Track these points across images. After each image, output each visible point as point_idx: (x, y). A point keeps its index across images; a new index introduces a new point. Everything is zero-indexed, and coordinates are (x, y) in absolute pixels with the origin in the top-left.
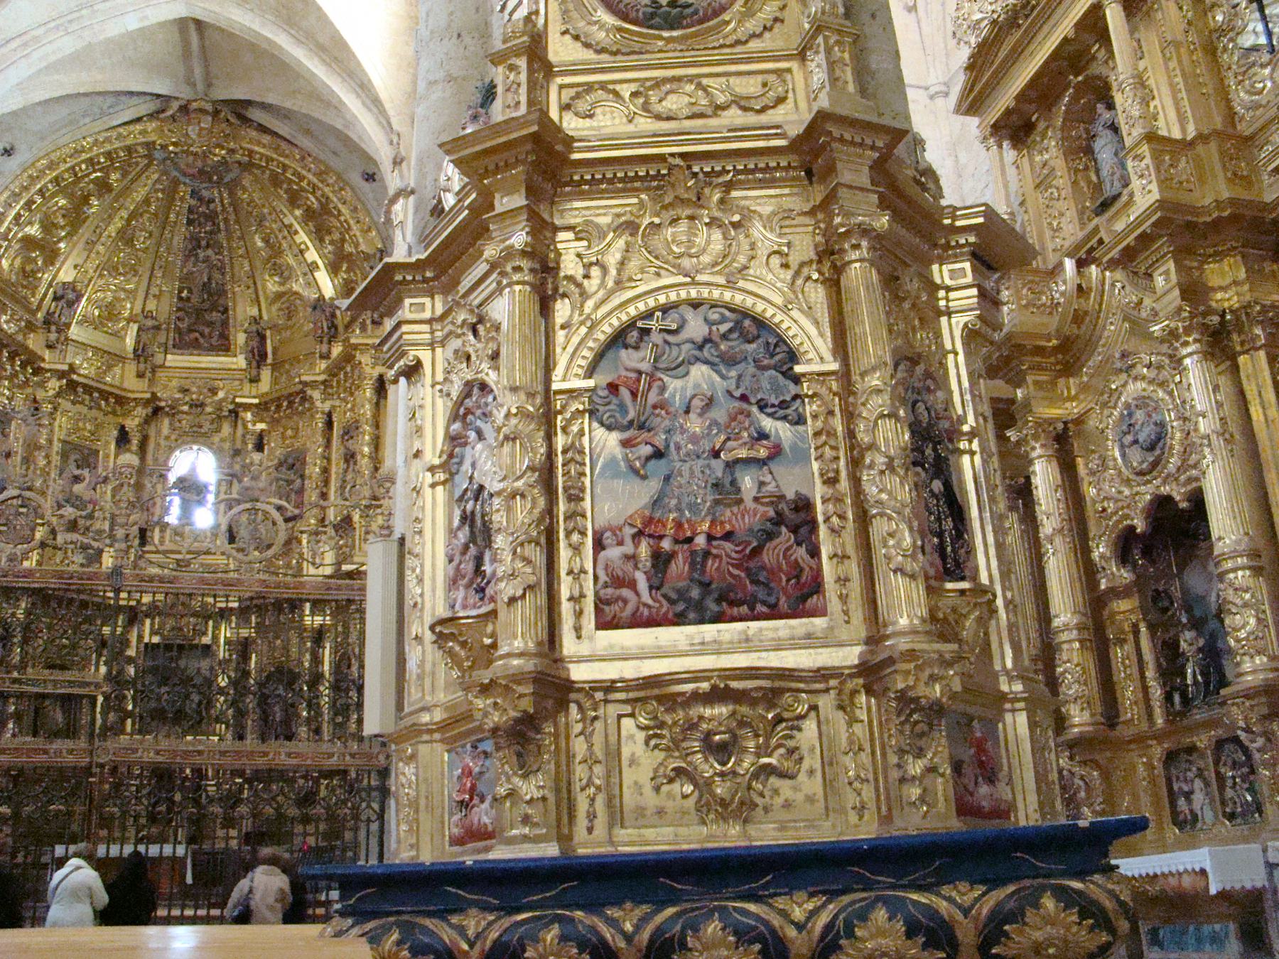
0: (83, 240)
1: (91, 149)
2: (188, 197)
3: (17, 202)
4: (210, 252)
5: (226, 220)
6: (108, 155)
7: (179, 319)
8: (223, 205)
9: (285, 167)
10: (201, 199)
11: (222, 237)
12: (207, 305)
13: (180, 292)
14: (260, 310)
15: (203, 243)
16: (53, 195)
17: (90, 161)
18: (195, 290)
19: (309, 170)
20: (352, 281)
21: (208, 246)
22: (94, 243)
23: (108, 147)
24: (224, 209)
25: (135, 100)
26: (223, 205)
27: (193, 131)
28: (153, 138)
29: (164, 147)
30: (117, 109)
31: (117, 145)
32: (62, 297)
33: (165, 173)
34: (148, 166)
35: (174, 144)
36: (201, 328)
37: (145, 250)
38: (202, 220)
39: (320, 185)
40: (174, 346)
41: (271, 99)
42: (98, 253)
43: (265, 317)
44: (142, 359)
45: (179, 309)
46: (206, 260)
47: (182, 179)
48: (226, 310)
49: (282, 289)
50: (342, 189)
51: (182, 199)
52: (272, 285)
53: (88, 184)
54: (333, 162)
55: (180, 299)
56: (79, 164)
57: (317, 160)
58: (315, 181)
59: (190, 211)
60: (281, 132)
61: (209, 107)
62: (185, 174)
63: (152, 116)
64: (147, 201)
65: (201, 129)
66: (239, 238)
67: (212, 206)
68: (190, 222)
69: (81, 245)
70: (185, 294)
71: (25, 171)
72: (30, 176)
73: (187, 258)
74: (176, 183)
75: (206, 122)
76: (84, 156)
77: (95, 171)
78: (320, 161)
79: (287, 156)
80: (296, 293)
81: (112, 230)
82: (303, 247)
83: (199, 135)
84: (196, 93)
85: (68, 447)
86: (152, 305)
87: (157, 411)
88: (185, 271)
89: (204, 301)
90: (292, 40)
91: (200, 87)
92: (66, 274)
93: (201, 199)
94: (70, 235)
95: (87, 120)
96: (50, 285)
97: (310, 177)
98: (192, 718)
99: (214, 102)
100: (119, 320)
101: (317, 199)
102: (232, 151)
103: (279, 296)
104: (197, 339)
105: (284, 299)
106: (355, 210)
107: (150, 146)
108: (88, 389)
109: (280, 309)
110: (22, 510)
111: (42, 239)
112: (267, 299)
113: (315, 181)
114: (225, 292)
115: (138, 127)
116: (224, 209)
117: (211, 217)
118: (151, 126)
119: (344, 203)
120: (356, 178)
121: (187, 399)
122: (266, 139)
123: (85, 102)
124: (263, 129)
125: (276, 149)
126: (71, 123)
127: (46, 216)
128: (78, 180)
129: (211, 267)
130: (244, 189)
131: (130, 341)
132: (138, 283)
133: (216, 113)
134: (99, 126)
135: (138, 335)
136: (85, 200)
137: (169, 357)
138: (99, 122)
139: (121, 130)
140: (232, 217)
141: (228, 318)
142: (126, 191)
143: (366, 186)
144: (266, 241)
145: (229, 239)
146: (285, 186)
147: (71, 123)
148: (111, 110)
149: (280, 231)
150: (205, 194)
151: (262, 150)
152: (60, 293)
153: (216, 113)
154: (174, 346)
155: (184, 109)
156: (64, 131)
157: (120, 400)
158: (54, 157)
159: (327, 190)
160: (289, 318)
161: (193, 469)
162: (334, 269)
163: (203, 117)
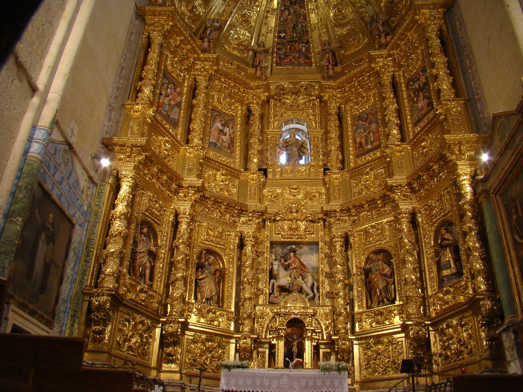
7: (279, 49)
36: (293, 54)
44: (259, 68)
45: (278, 44)
48: (307, 43)
73: (282, 12)
85: (216, 113)
98: (307, 294)
104: (291, 60)
114: (307, 31)
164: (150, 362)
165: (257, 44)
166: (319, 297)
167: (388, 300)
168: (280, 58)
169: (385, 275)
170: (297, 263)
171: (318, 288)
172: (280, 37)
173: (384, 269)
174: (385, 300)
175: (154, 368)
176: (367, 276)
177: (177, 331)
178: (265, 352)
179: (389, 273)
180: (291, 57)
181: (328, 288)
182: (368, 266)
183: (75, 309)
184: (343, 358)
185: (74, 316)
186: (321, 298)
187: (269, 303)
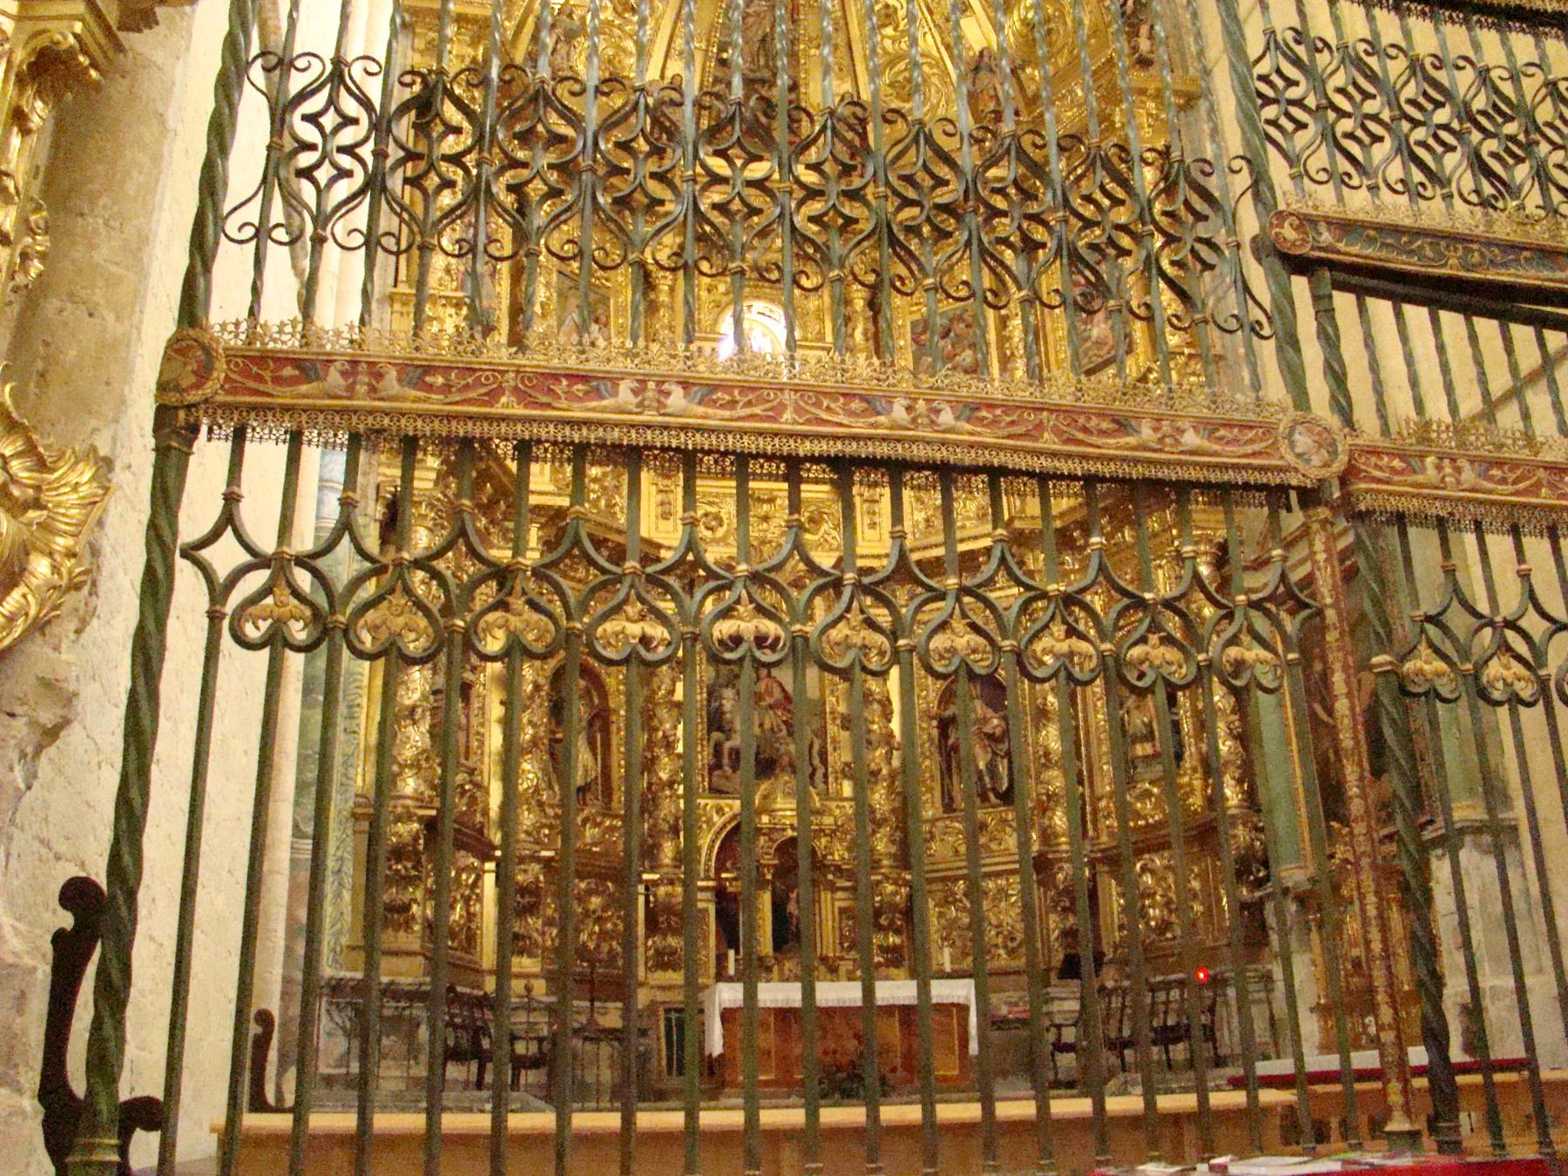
164: (477, 958)
165: (662, 77)
166: (826, 776)
167: (998, 795)
169: (990, 736)
170: (777, 694)
171: (823, 756)
173: (985, 720)
174: (992, 796)
175: (490, 972)
176: (944, 735)
177: (537, 879)
178: (706, 910)
179: (998, 731)
181: (847, 757)
182: (948, 713)
183: (339, 853)
184: (892, 922)
185: (339, 871)
186: (831, 779)
187: (710, 788)
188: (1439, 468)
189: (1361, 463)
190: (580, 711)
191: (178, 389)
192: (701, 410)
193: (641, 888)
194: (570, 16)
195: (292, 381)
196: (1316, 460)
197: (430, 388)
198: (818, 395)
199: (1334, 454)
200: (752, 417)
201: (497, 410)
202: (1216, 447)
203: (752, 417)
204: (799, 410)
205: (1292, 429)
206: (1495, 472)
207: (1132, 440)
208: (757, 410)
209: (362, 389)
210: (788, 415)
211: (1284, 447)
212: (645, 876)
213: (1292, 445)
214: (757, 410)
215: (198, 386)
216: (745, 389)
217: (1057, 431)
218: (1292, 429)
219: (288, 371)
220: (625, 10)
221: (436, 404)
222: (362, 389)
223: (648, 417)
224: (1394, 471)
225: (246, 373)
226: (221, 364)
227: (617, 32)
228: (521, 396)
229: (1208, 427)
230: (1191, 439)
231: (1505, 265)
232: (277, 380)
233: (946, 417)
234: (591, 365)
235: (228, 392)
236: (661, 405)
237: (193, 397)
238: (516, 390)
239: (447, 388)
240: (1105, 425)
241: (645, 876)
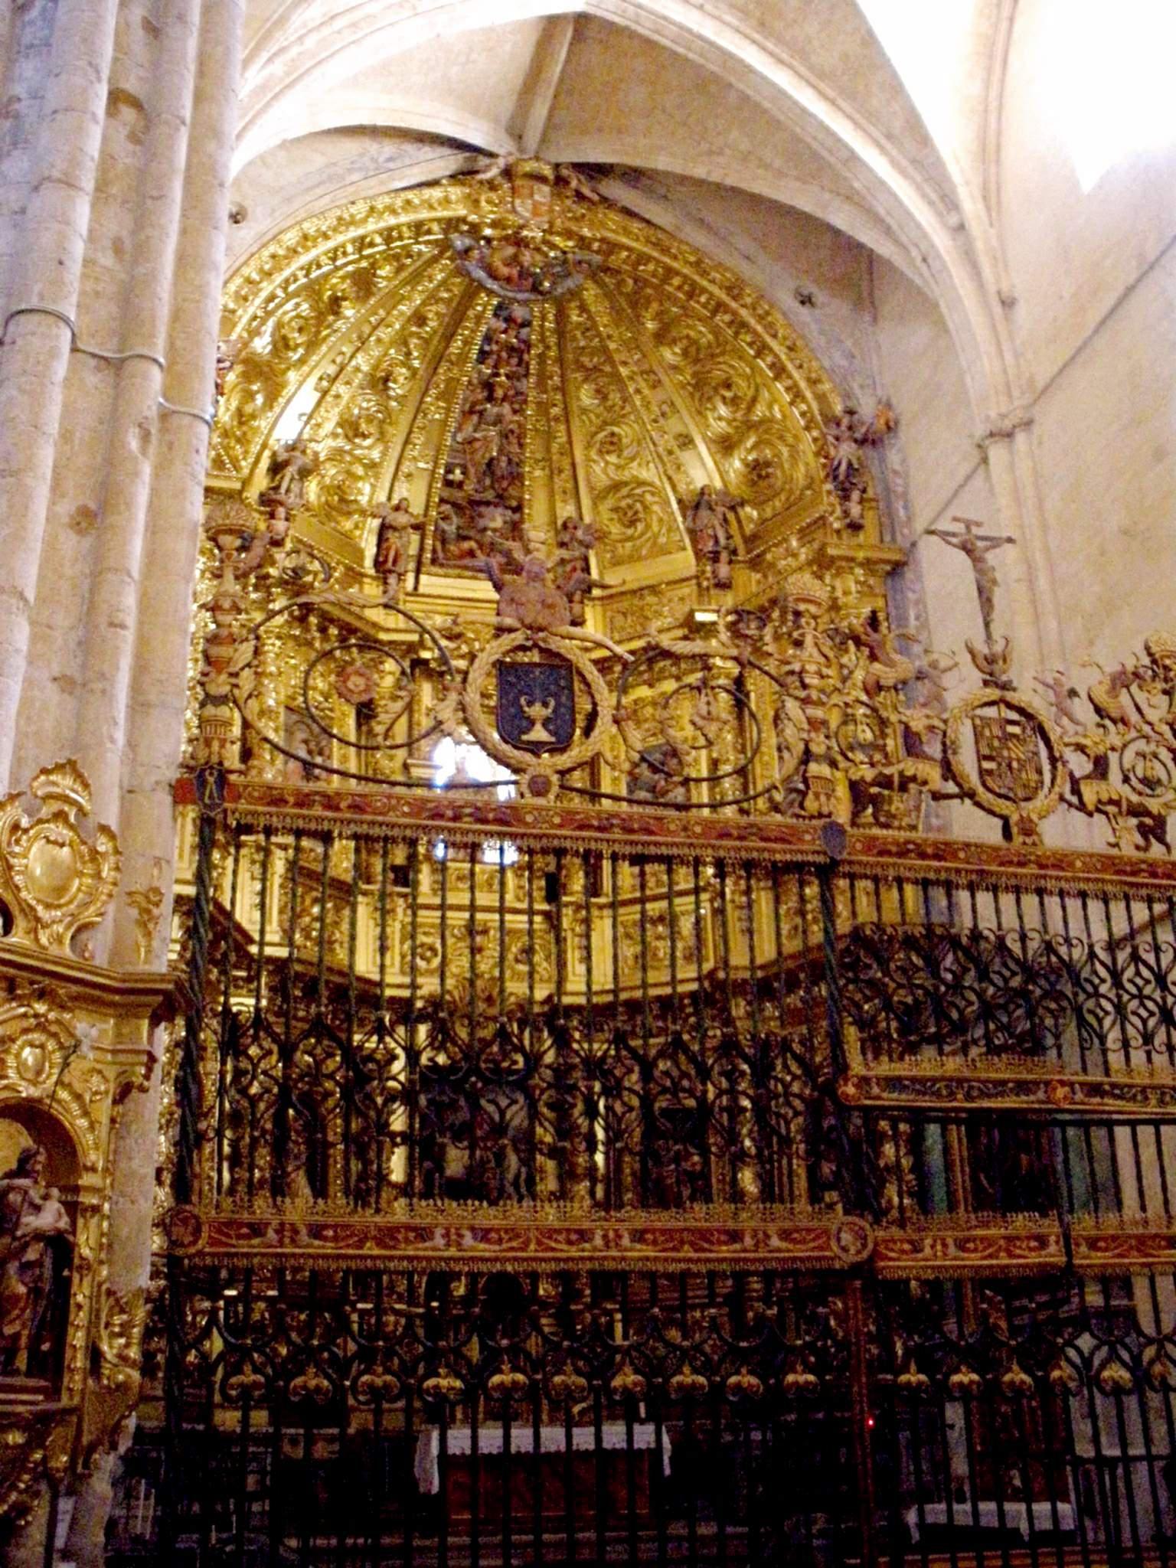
0: (317, 374)
1: (365, 220)
2: (489, 314)
3: (256, 294)
4: (506, 409)
5: (542, 358)
6: (388, 235)
8: (542, 334)
9: (670, 272)
10: (509, 320)
11: (529, 384)
12: (490, 495)
13: (449, 470)
14: (579, 508)
15: (499, 393)
16: (296, 294)
17: (361, 243)
18: (472, 471)
19: (713, 281)
20: (768, 464)
21: (504, 399)
22: (333, 380)
23: (392, 221)
24: (543, 340)
25: (427, 152)
26: (542, 334)
27: (524, 208)
28: (461, 212)
29: (474, 230)
30: (398, 164)
31: (404, 218)
32: (286, 463)
33: (461, 272)
34: (435, 259)
35: (494, 225)
37: (401, 400)
38: (504, 355)
39: (733, 305)
40: (434, 561)
41: (661, 162)
42: (337, 396)
43: (587, 519)
45: (442, 501)
46: (499, 420)
47: (491, 284)
48: (518, 509)
49: (617, 476)
50: (768, 313)
51: (479, 318)
52: (600, 470)
53: (343, 278)
54: (746, 270)
55: (448, 483)
56: (343, 246)
57: (719, 266)
58: (723, 296)
59: (488, 339)
60: (655, 220)
61: (547, 171)
62: (493, 275)
63: (460, 177)
64: (420, 319)
65: (536, 205)
66: (556, 389)
67: (525, 331)
68: (483, 356)
69: (312, 380)
70: (457, 475)
71: (264, 246)
72: (273, 256)
74: (473, 289)
75: (543, 193)
76: (354, 232)
77: (362, 257)
78: (727, 269)
79: (675, 258)
80: (651, 484)
81: (362, 361)
82: (665, 408)
83: (535, 213)
84: (521, 150)
85: (295, 717)
86: (402, 491)
87: (419, 663)
88: (459, 438)
89: (485, 489)
90: (771, 60)
91: (532, 139)
92: (286, 428)
93: (509, 320)
94: (302, 361)
95: (355, 177)
96: (264, 446)
97: (715, 290)
99: (557, 166)
100: (349, 514)
101: (716, 332)
102: (583, 243)
103: (616, 486)
105: (625, 491)
106: (791, 349)
107: (451, 225)
108: (326, 620)
109: (616, 510)
110: (1011, 729)
111: (269, 364)
112: (592, 489)
113: (723, 296)
115: (436, 193)
116: (543, 340)
117: (518, 352)
118: (456, 192)
119: (775, 336)
120: (787, 300)
121: (465, 649)
122: (635, 226)
123: (351, 147)
124: (628, 213)
125: (655, 245)
126: (330, 178)
127: (279, 326)
128: (337, 269)
129: (505, 435)
130: (583, 308)
131: (370, 550)
132: (384, 454)
133: (560, 181)
134: (373, 186)
135: (381, 539)
136: (336, 303)
137: (423, 578)
138: (373, 182)
139: (410, 195)
140: (553, 353)
141: (522, 521)
142: (393, 299)
143: (804, 312)
144: (601, 394)
145: (541, 385)
146: (655, 306)
147: (330, 178)
148: (391, 165)
149: (631, 378)
150: (519, 312)
151: (634, 244)
152: (283, 456)
153: (560, 181)
154: (434, 561)
155: (508, 173)
156: (319, 191)
157: (369, 644)
158: (310, 227)
159: (743, 312)
160: (632, 523)
161: (460, 770)
162: (726, 445)
163: (537, 186)
165: (389, 499)
168: (444, 542)
172: (448, 483)
180: (473, 544)
188: (933, 1247)
189: (882, 1249)
190: (297, 1146)
191: (182, 1245)
192: (482, 1246)
193: (355, 1317)
194: (304, 452)
195: (247, 1237)
196: (853, 1251)
197: (325, 1239)
198: (551, 1233)
199: (864, 1246)
200: (512, 1249)
201: (364, 1252)
202: (791, 1246)
203: (512, 1249)
204: (539, 1243)
205: (840, 1230)
206: (971, 1245)
207: (737, 1246)
208: (514, 1244)
209: (287, 1241)
210: (532, 1246)
211: (833, 1244)
212: (360, 1306)
213: (839, 1240)
214: (514, 1244)
215: (194, 1243)
216: (506, 1231)
217: (692, 1244)
218: (840, 1230)
219: (245, 1230)
220: (356, 436)
221: (329, 1249)
222: (287, 1241)
223: (452, 1252)
224: (903, 1252)
225: (219, 1231)
226: (205, 1228)
227: (348, 458)
228: (380, 1243)
229: (785, 1235)
230: (775, 1242)
231: (996, 1095)
232: (239, 1237)
233: (626, 1241)
234: (418, 1221)
235: (211, 1245)
236: (459, 1244)
237: (192, 1250)
238: (374, 1238)
239: (335, 1239)
240: (723, 1238)
241: (360, 1306)
